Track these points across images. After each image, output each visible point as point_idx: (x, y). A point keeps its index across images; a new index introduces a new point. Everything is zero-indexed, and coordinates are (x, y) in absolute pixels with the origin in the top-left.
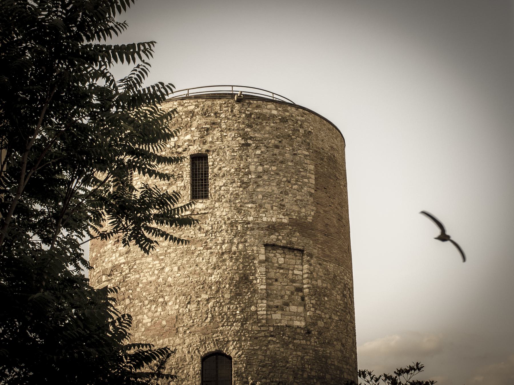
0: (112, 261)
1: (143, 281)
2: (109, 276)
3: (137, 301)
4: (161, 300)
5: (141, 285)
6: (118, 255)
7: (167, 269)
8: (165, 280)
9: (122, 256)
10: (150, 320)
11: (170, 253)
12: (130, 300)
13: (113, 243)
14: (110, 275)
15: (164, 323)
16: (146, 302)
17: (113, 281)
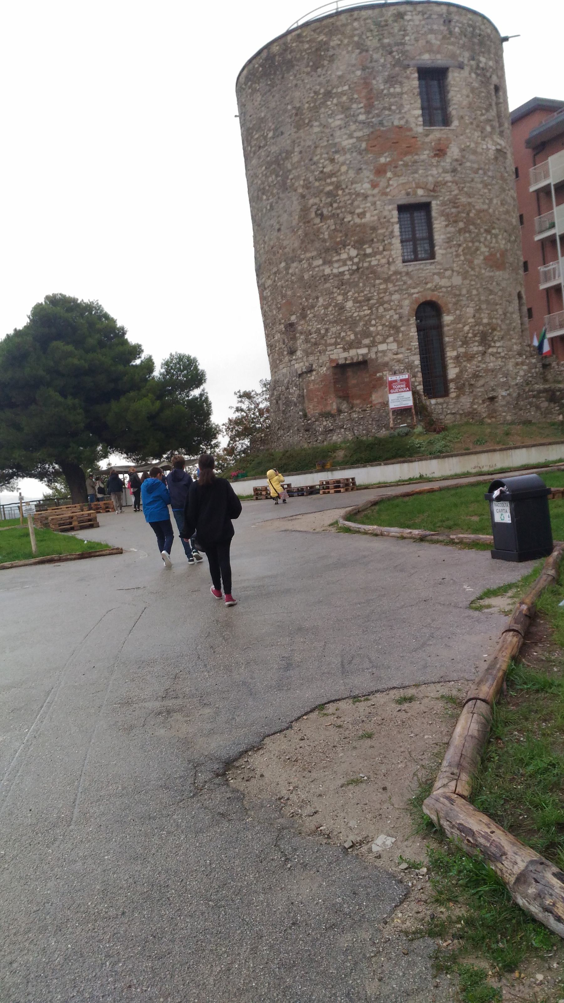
0: (432, 176)
1: (477, 207)
2: (431, 191)
3: (471, 227)
4: (493, 231)
5: (473, 211)
6: (440, 170)
7: (495, 201)
8: (494, 211)
9: (447, 172)
10: (487, 250)
11: (494, 185)
12: (465, 223)
13: (432, 154)
14: (434, 191)
15: (498, 255)
16: (482, 230)
17: (441, 198)
